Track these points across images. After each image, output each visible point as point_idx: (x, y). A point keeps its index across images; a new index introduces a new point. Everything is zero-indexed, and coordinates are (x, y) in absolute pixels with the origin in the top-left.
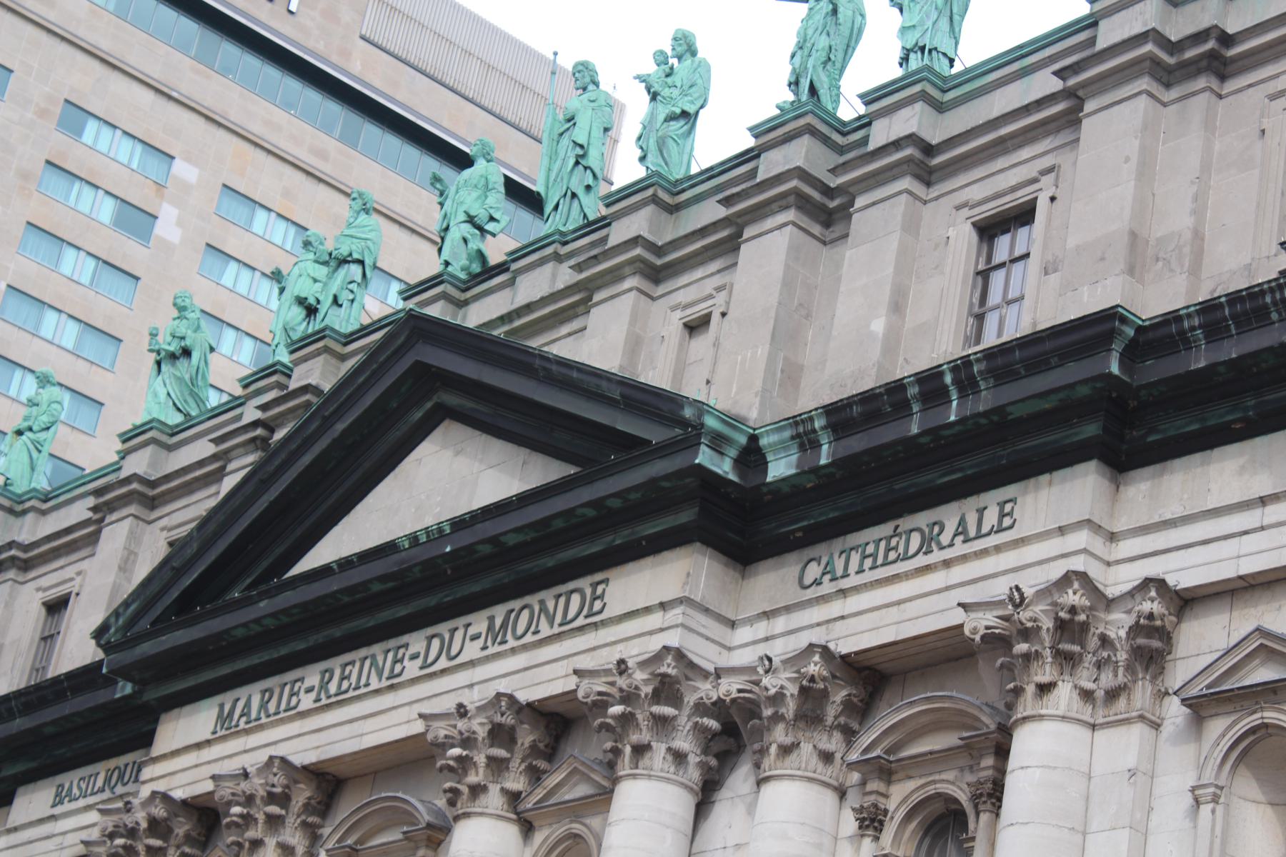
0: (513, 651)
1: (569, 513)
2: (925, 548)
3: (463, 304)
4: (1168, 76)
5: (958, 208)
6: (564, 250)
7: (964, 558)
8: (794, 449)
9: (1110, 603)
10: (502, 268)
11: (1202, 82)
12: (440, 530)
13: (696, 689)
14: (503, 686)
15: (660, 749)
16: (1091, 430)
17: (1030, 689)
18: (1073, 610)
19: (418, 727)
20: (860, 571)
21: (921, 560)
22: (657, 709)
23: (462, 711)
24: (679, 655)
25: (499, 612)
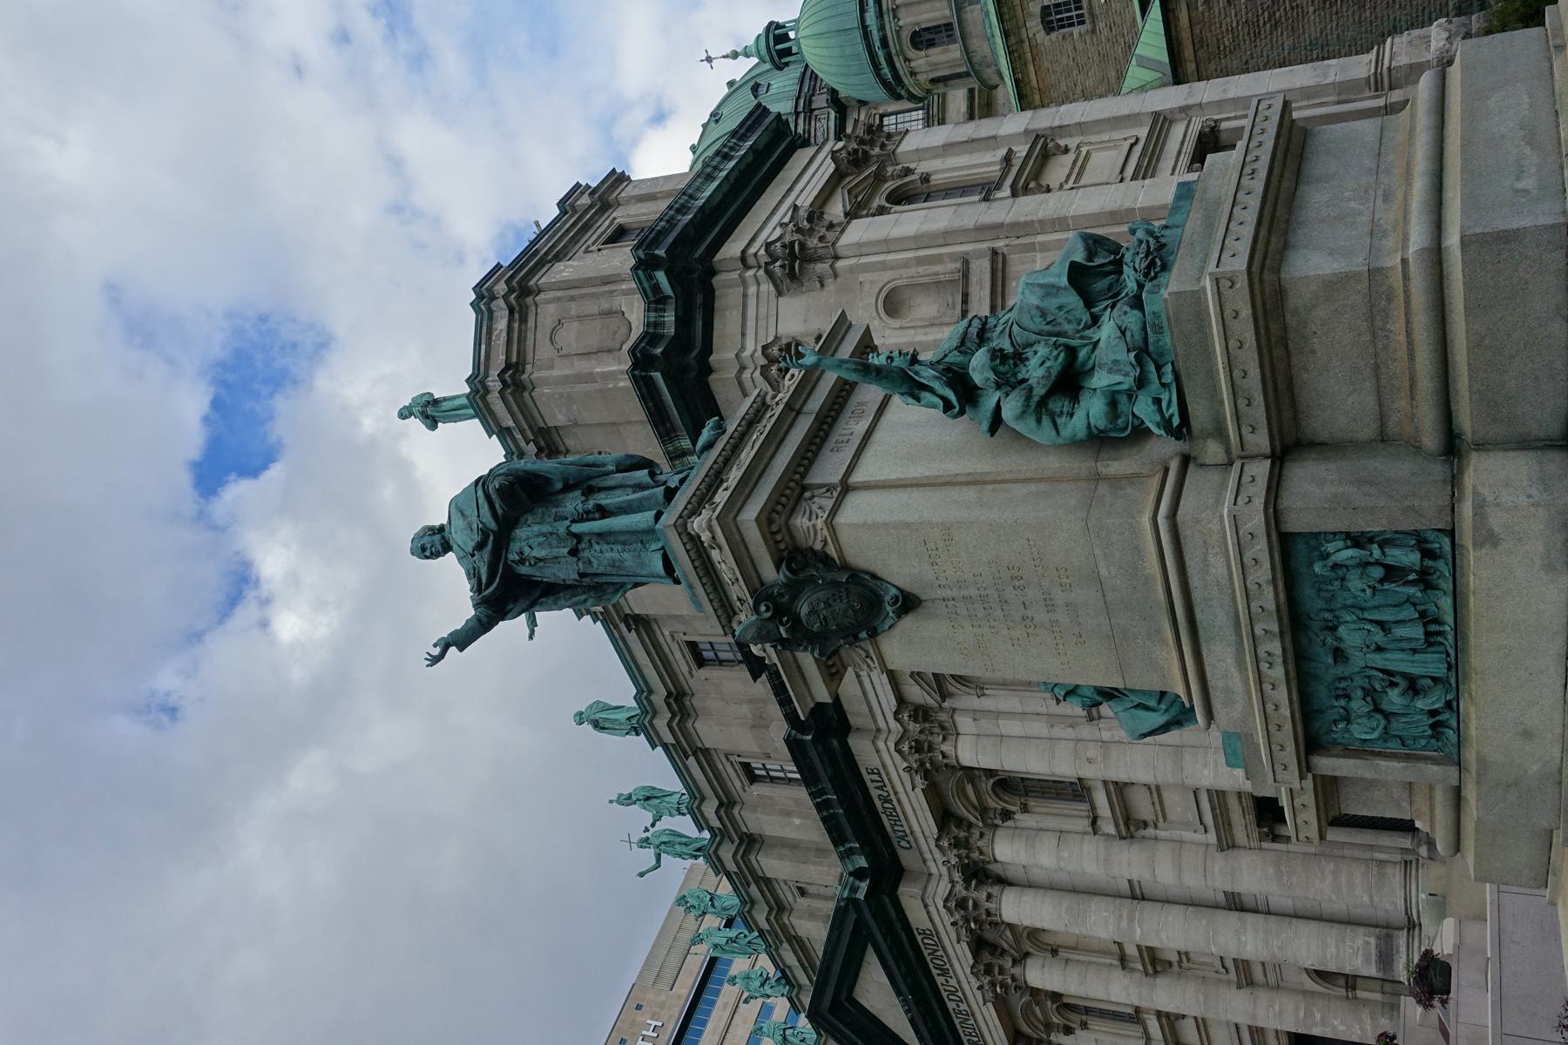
0: (952, 966)
1: (889, 947)
2: (890, 801)
3: (799, 986)
5: (745, 791)
7: (893, 787)
8: (853, 857)
9: (905, 731)
10: (783, 972)
11: (688, 703)
12: (902, 1001)
13: (960, 891)
14: (968, 971)
15: (988, 905)
16: (835, 743)
17: (945, 761)
18: (911, 748)
19: (990, 1005)
20: (902, 826)
21: (895, 803)
22: (971, 909)
23: (980, 988)
24: (946, 901)
25: (935, 972)
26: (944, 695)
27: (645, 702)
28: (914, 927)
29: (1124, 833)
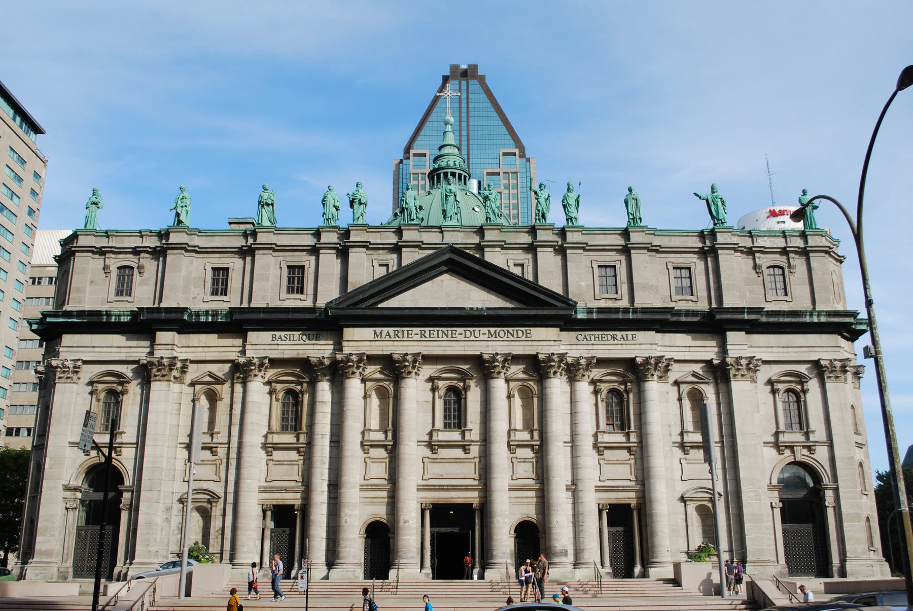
4: (649, 250)
6: (461, 230)
25: (492, 330)
26: (677, 383)
27: (652, 232)
28: (532, 329)
29: (599, 445)
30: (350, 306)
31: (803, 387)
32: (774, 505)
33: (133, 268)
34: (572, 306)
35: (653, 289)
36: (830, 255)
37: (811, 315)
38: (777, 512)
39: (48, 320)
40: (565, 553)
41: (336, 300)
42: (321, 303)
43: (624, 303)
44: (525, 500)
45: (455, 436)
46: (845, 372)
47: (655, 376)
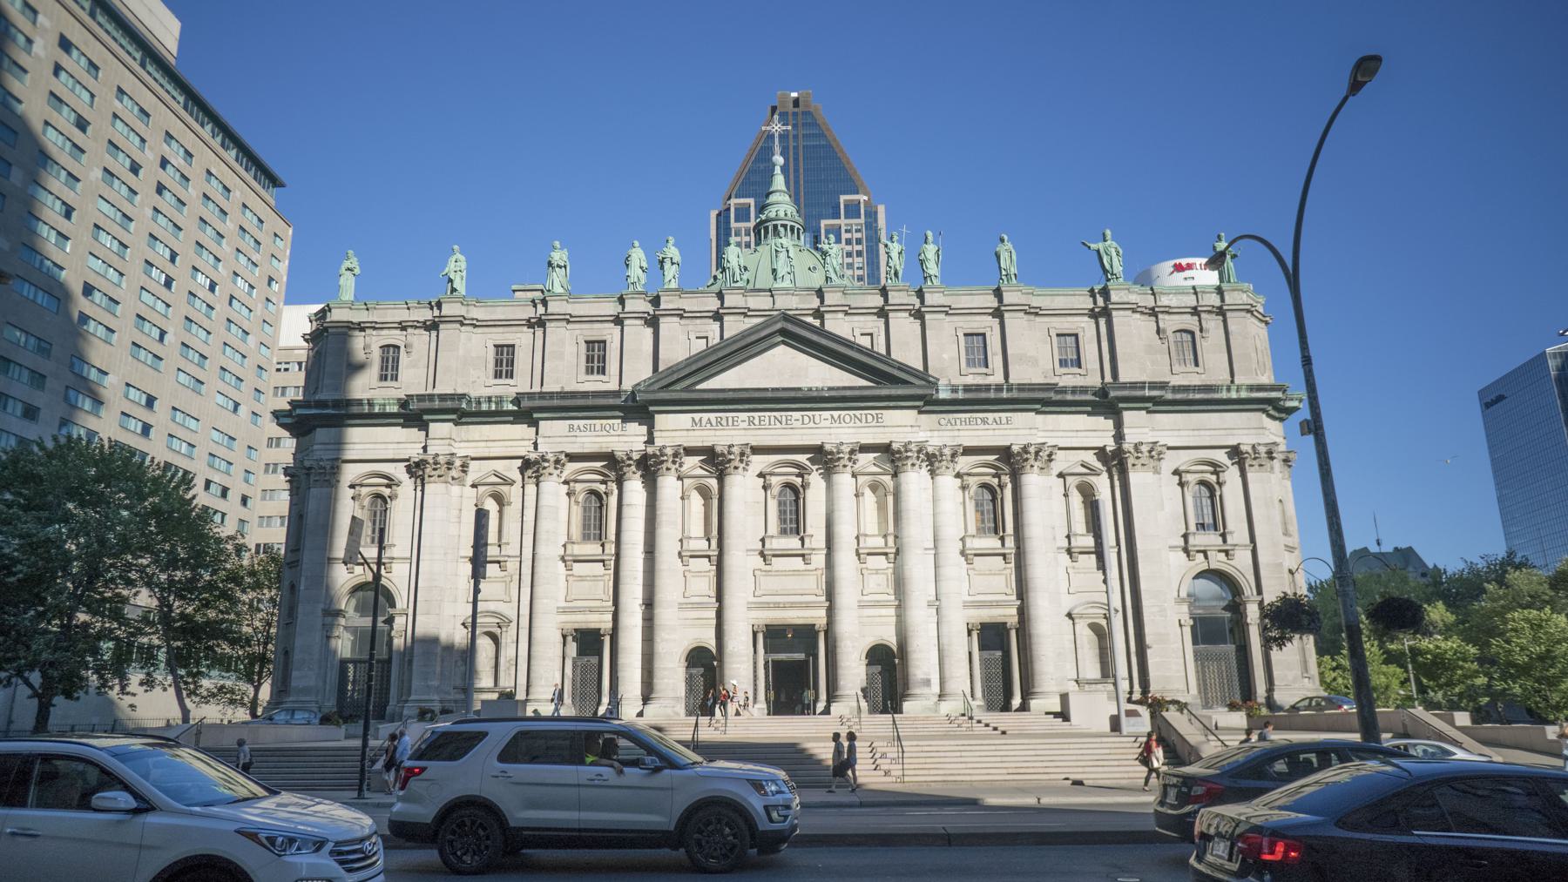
4: (1026, 313)
25: (835, 414)
26: (1061, 475)
30: (662, 388)
31: (1218, 478)
32: (1182, 622)
33: (398, 347)
34: (934, 384)
35: (1034, 362)
36: (1252, 314)
37: (1229, 390)
38: (1187, 631)
39: (299, 411)
40: (927, 683)
41: (645, 381)
42: (628, 385)
43: (998, 378)
44: (878, 619)
45: (793, 543)
46: (1272, 458)
47: (1035, 467)
